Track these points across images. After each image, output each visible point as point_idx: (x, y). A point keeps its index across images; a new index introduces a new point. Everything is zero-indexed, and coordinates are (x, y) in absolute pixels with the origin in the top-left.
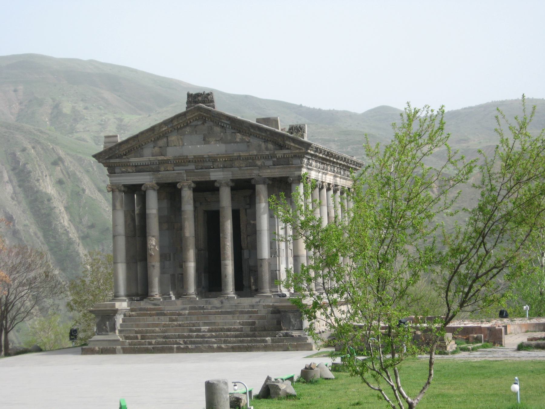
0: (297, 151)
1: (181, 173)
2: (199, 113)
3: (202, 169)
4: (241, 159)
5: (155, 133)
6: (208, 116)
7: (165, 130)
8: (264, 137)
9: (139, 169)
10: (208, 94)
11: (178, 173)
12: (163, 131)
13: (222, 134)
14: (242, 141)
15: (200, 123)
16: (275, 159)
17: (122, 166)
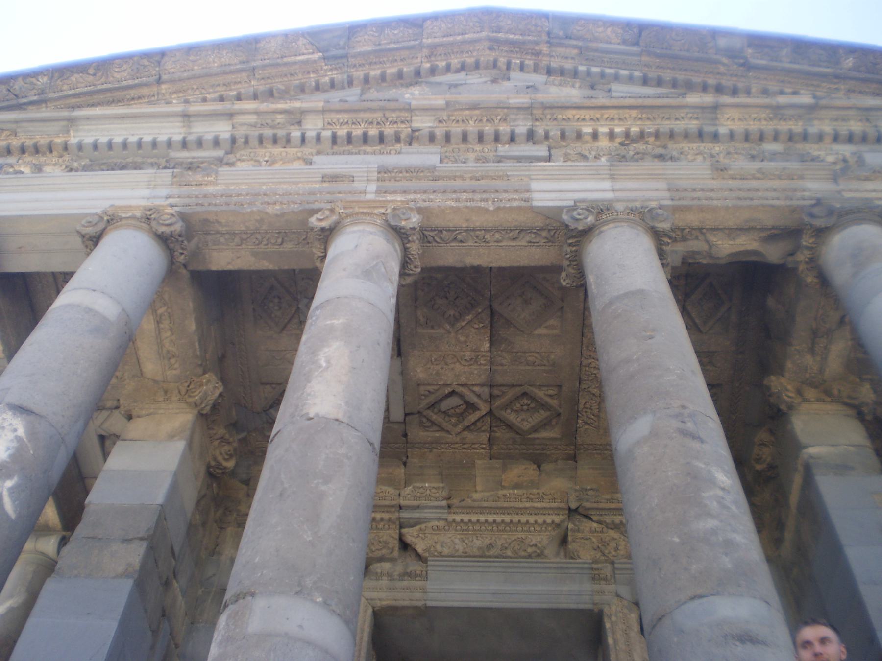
2: (484, 34)
4: (723, 130)
6: (530, 38)
11: (334, 178)
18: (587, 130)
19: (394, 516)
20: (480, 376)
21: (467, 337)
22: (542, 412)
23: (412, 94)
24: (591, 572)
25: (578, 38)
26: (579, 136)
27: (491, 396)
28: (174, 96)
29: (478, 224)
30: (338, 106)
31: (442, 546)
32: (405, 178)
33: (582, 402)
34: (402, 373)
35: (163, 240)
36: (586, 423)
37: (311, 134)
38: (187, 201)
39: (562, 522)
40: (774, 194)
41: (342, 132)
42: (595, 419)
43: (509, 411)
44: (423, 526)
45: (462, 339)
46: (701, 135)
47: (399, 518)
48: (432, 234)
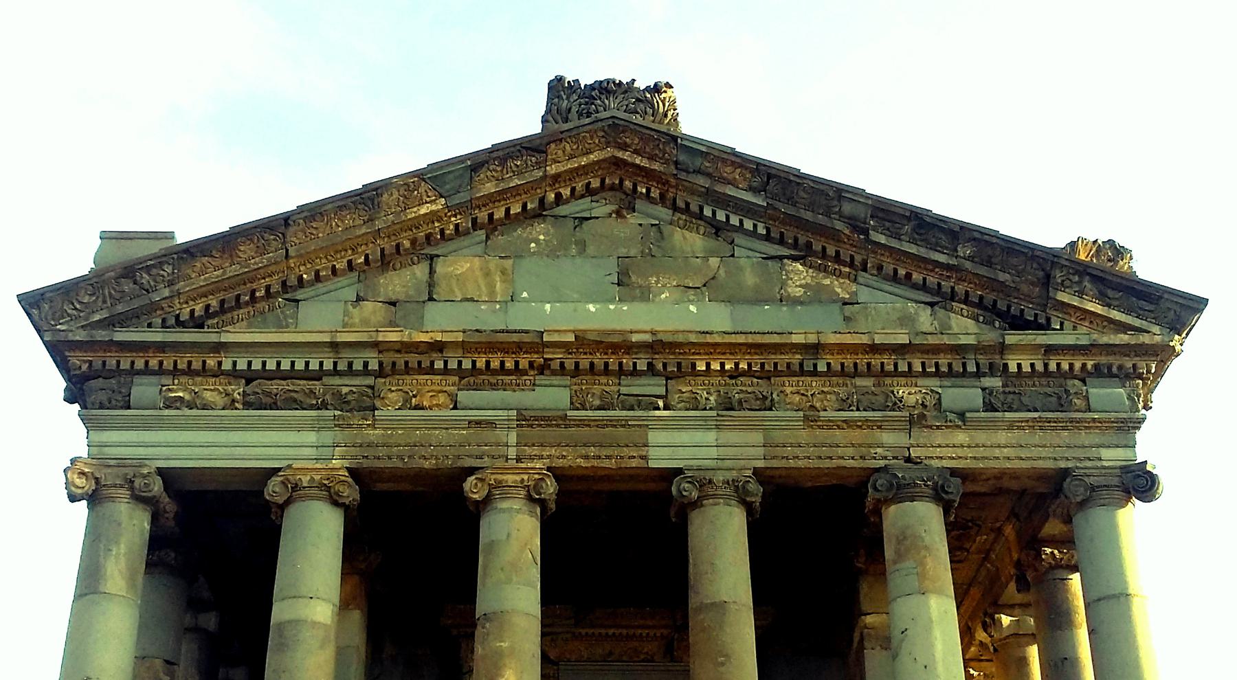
0: (1123, 338)
1: (491, 424)
2: (609, 152)
3: (599, 408)
4: (822, 367)
5: (379, 224)
6: (656, 166)
7: (433, 217)
8: (932, 280)
9: (264, 391)
10: (657, 89)
11: (478, 423)
12: (416, 224)
13: (714, 262)
14: (816, 296)
15: (601, 209)
16: (995, 382)
17: (175, 372)
18: (701, 367)
23: (537, 241)
25: (709, 175)
26: (694, 365)
28: (302, 268)
30: (477, 338)
32: (540, 425)
35: (346, 508)
37: (453, 365)
38: (353, 451)
40: (850, 451)
41: (481, 364)
46: (802, 372)
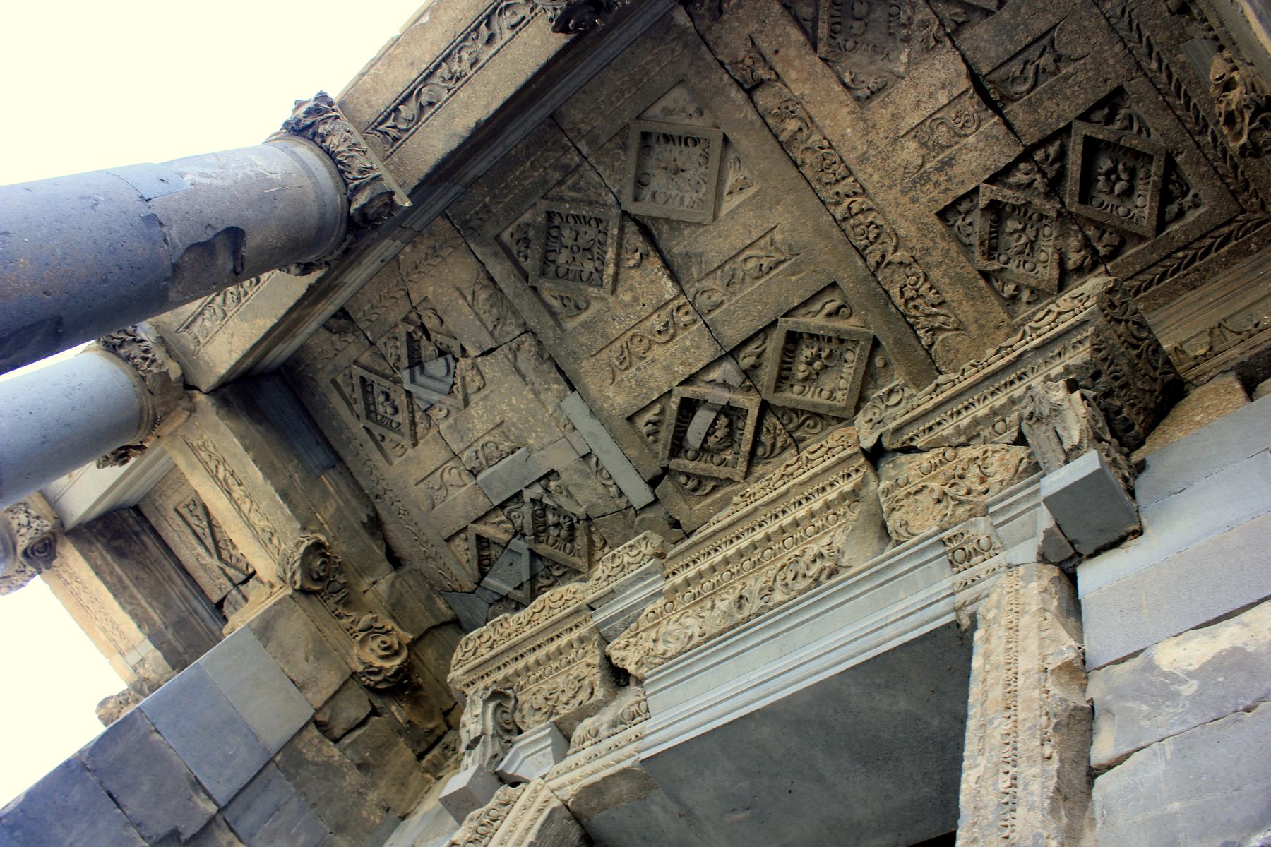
19: (583, 631)
20: (698, 347)
21: (632, 289)
22: (849, 356)
24: (942, 550)
27: (748, 373)
29: (428, 59)
31: (666, 642)
33: (894, 292)
34: (591, 412)
36: (934, 330)
39: (864, 482)
42: (943, 311)
43: (797, 388)
44: (633, 626)
45: (627, 298)
47: (597, 628)
48: (390, 123)
